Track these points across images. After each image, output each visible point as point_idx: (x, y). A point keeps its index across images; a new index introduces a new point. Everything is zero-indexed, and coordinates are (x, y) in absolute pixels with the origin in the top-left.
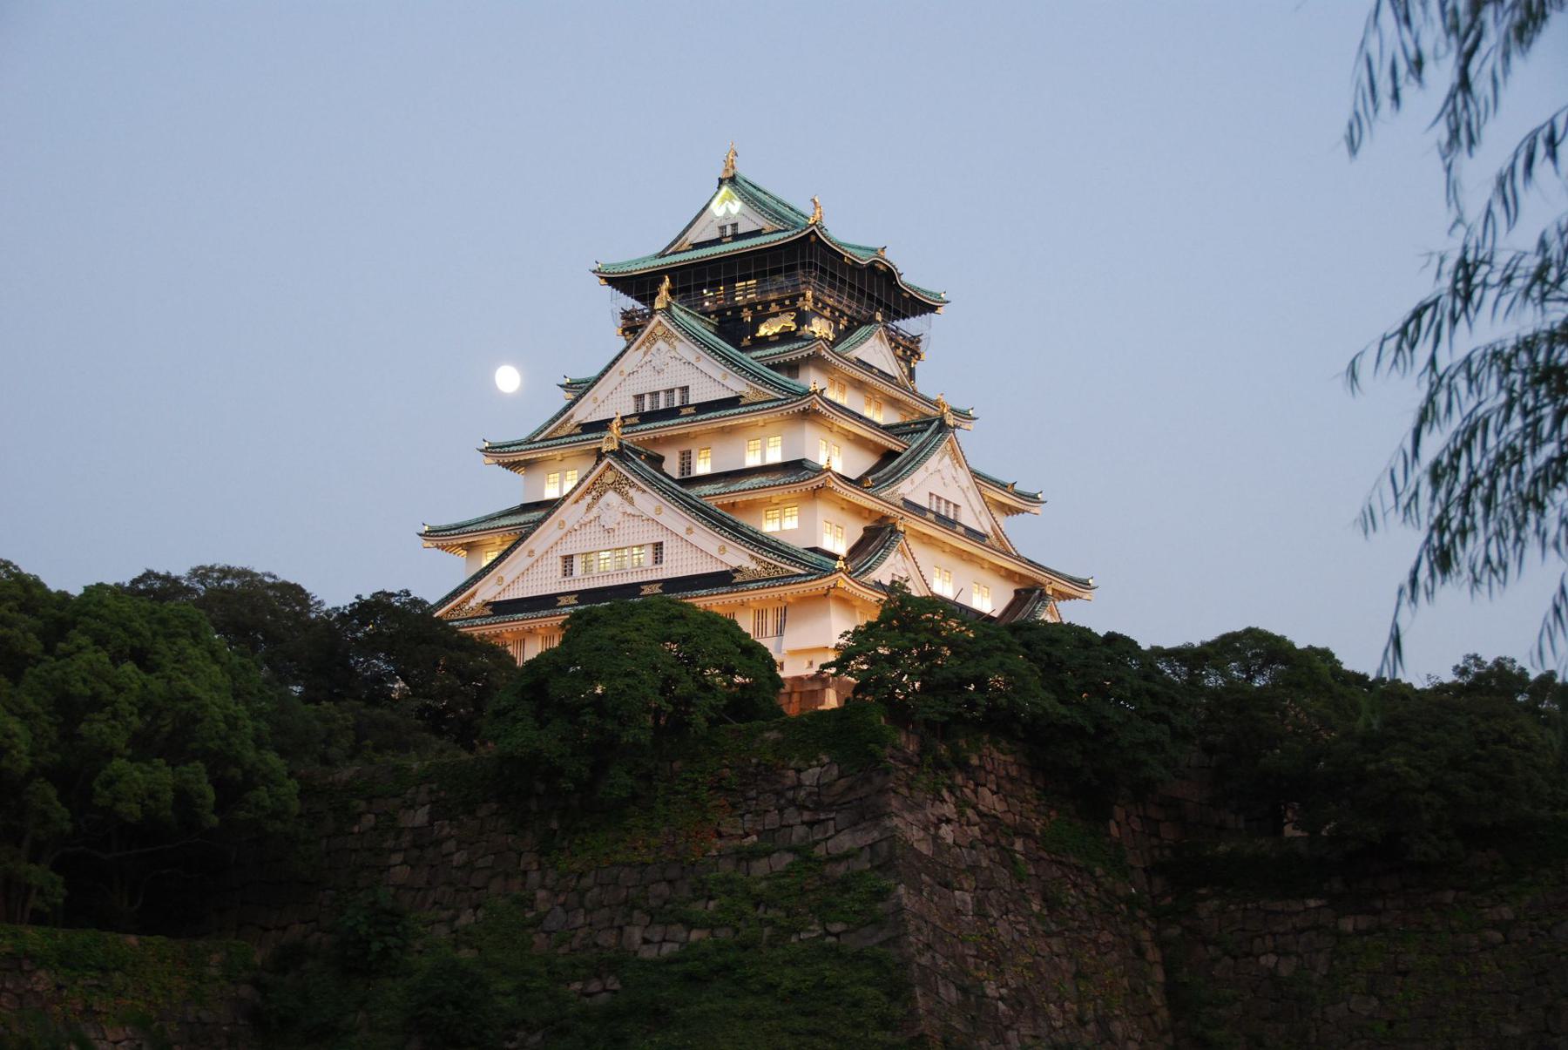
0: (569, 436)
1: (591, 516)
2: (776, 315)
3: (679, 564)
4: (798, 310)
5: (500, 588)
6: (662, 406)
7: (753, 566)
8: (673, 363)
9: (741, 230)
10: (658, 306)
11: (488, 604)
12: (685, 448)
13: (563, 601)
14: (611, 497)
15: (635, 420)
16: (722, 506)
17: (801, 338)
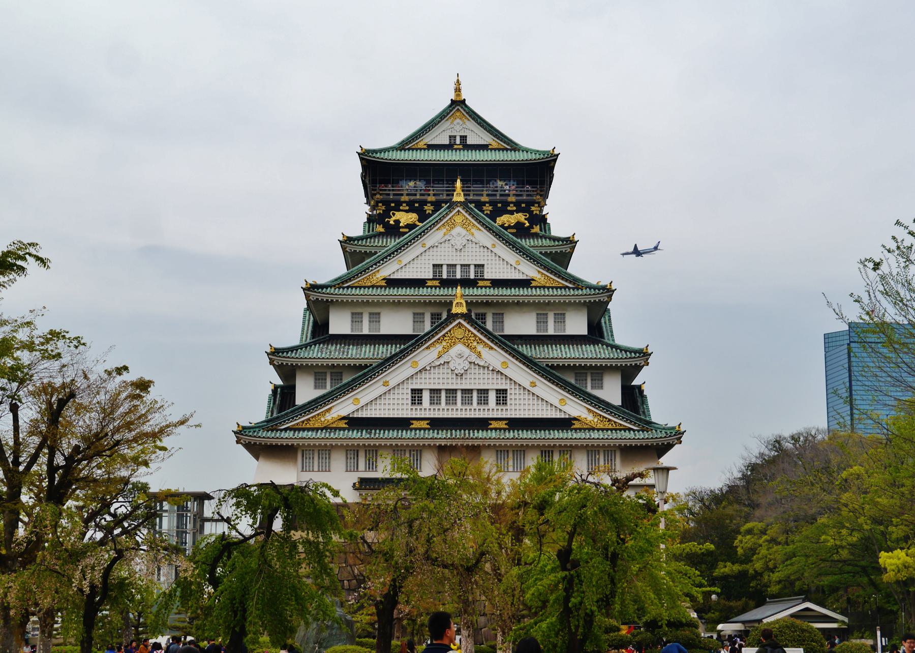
0: (373, 287)
1: (442, 361)
2: (511, 213)
3: (520, 407)
4: (531, 213)
5: (355, 408)
6: (458, 276)
7: (590, 417)
8: (470, 245)
9: (469, 142)
10: (456, 198)
11: (344, 418)
12: (481, 311)
13: (416, 424)
14: (459, 348)
15: (436, 283)
16: (552, 367)
17: (536, 236)
